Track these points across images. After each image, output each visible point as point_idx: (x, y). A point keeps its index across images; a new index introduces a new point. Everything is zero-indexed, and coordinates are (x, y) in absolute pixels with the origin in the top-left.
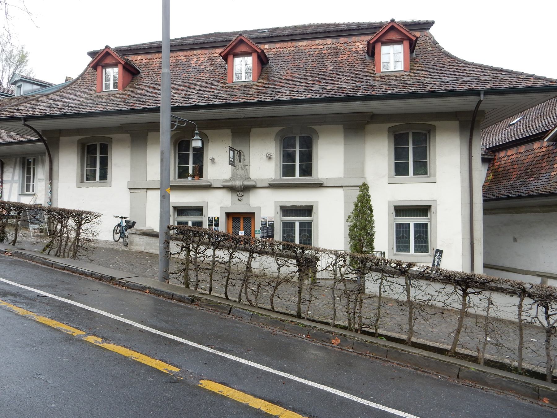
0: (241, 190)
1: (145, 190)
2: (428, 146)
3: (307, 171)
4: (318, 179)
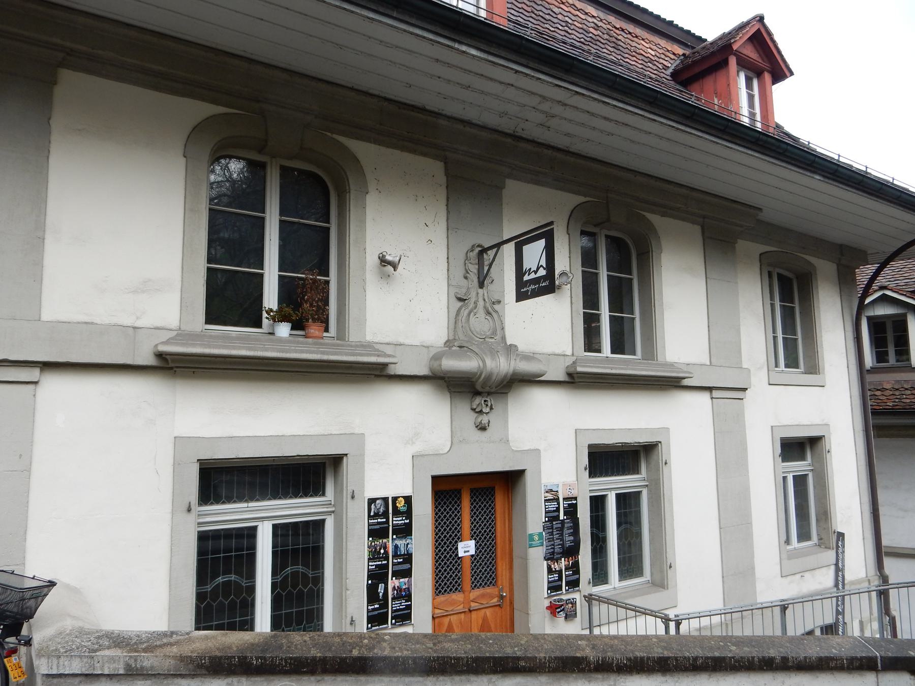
0: (475, 390)
1: (33, 374)
2: (635, 277)
3: (305, 305)
4: (369, 347)
